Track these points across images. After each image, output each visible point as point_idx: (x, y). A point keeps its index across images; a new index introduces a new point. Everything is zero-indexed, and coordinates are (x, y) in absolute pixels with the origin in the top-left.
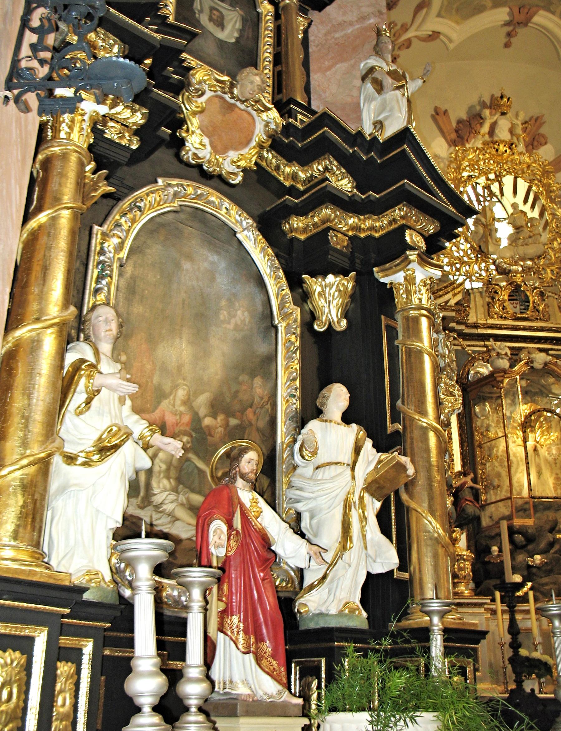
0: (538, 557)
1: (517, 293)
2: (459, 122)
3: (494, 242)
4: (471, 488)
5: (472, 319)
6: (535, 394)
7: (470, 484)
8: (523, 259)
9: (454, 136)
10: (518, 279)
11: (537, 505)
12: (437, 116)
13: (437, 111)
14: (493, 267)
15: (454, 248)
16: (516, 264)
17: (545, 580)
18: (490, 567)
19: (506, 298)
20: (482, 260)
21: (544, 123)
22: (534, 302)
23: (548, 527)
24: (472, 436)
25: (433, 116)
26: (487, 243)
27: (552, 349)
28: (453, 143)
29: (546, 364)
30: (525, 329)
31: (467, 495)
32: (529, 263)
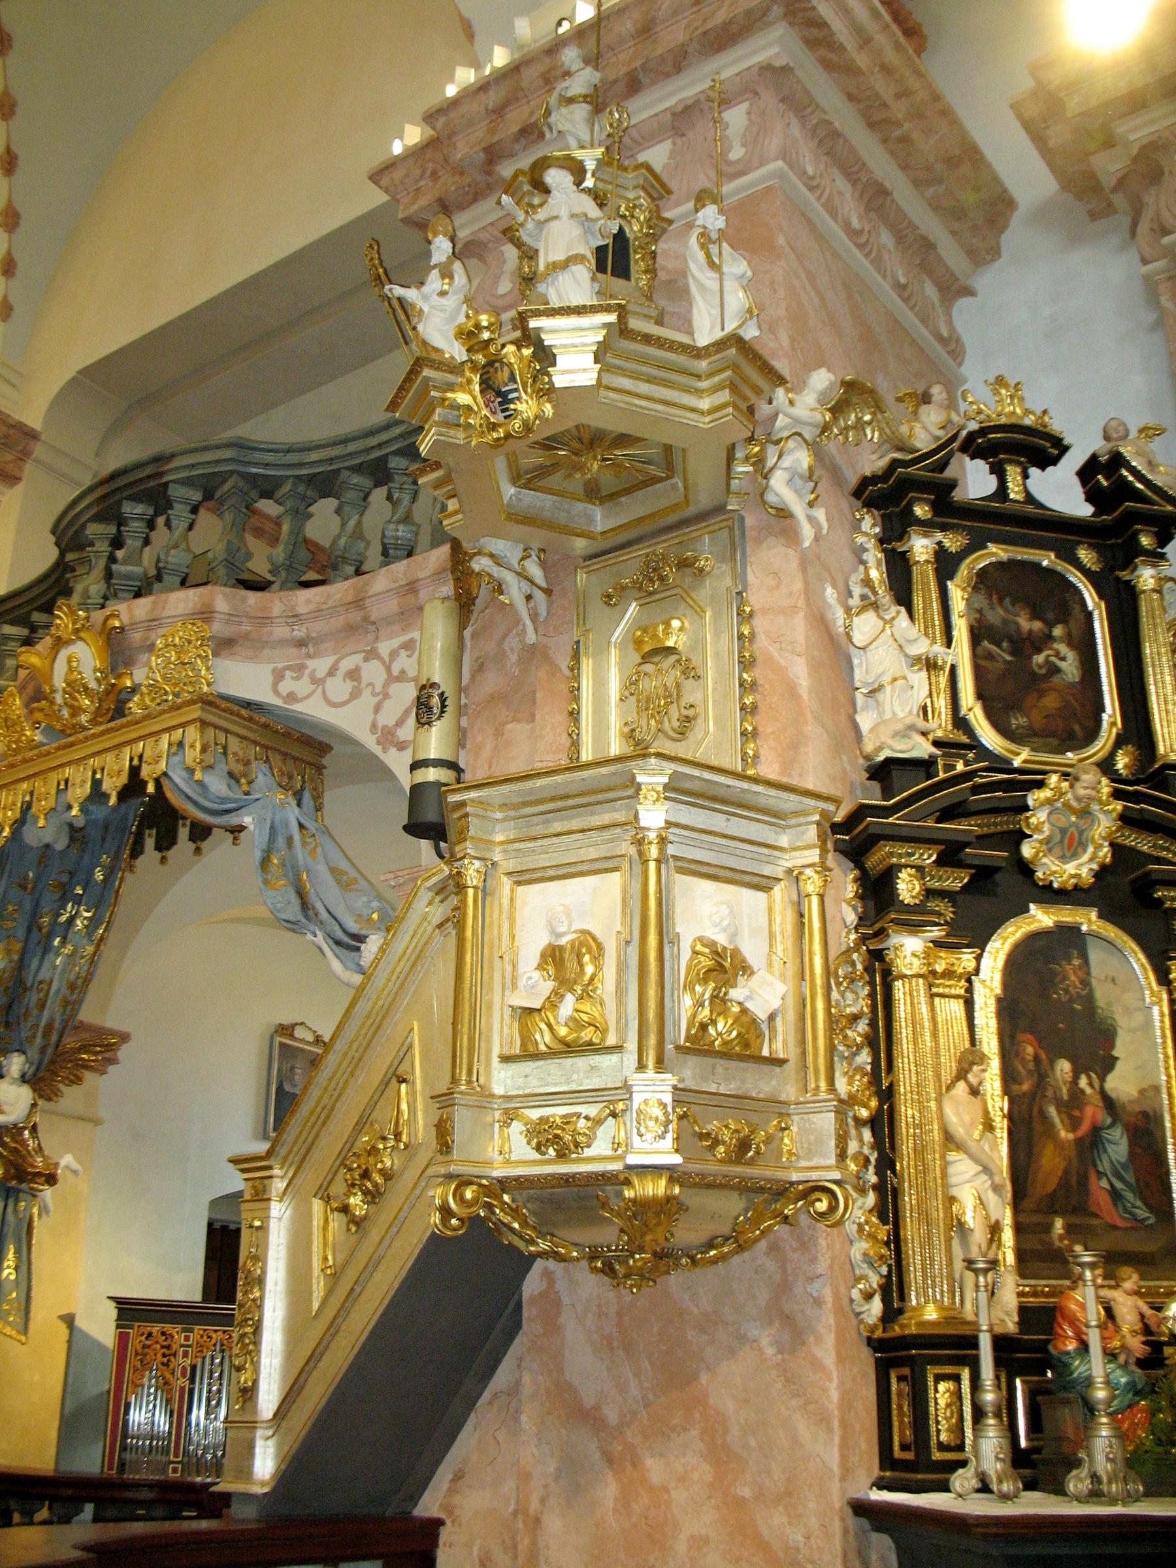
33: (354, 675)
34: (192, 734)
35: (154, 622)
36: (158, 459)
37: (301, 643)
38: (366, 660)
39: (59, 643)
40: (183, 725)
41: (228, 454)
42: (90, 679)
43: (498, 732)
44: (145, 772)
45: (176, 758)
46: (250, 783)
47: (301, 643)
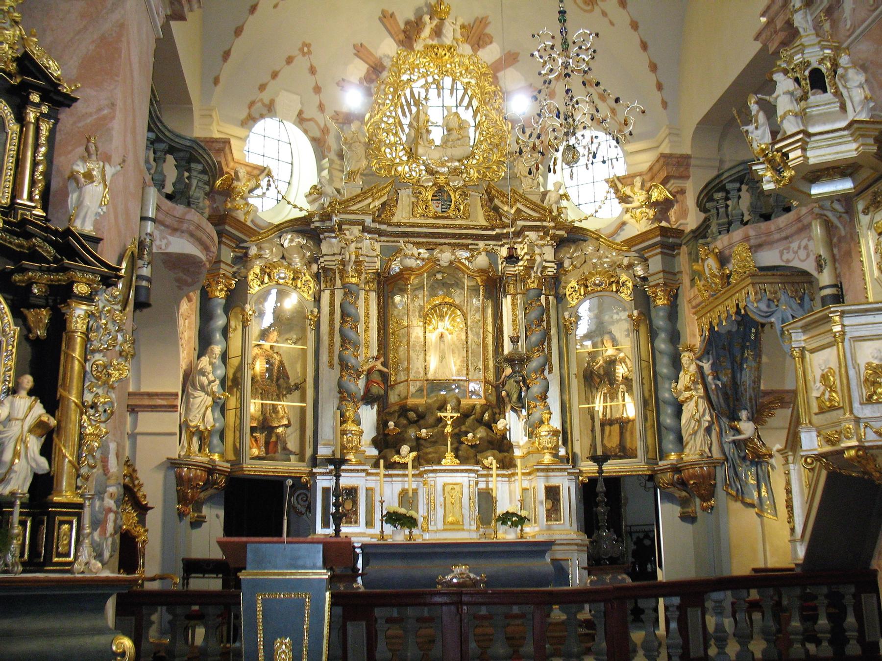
0: (424, 431)
1: (440, 192)
2: (407, 23)
3: (426, 144)
4: (380, 371)
5: (395, 220)
6: (452, 285)
7: (379, 366)
8: (451, 160)
9: (402, 36)
10: (441, 180)
11: (436, 385)
12: (384, 20)
13: (383, 12)
14: (423, 168)
15: (388, 150)
16: (443, 165)
17: (430, 450)
18: (389, 438)
19: (430, 198)
20: (414, 162)
21: (489, 23)
22: (456, 202)
23: (437, 405)
24: (388, 325)
25: (380, 19)
26: (417, 144)
27: (472, 244)
28: (401, 43)
29: (451, 263)
30: (444, 227)
31: (376, 377)
32: (457, 164)
33: (806, 247)
34: (751, 289)
35: (731, 246)
36: (718, 176)
37: (786, 238)
38: (809, 240)
39: (703, 260)
40: (747, 286)
41: (741, 167)
42: (715, 271)
43: (849, 268)
44: (740, 306)
45: (749, 298)
46: (778, 301)
47: (786, 238)
